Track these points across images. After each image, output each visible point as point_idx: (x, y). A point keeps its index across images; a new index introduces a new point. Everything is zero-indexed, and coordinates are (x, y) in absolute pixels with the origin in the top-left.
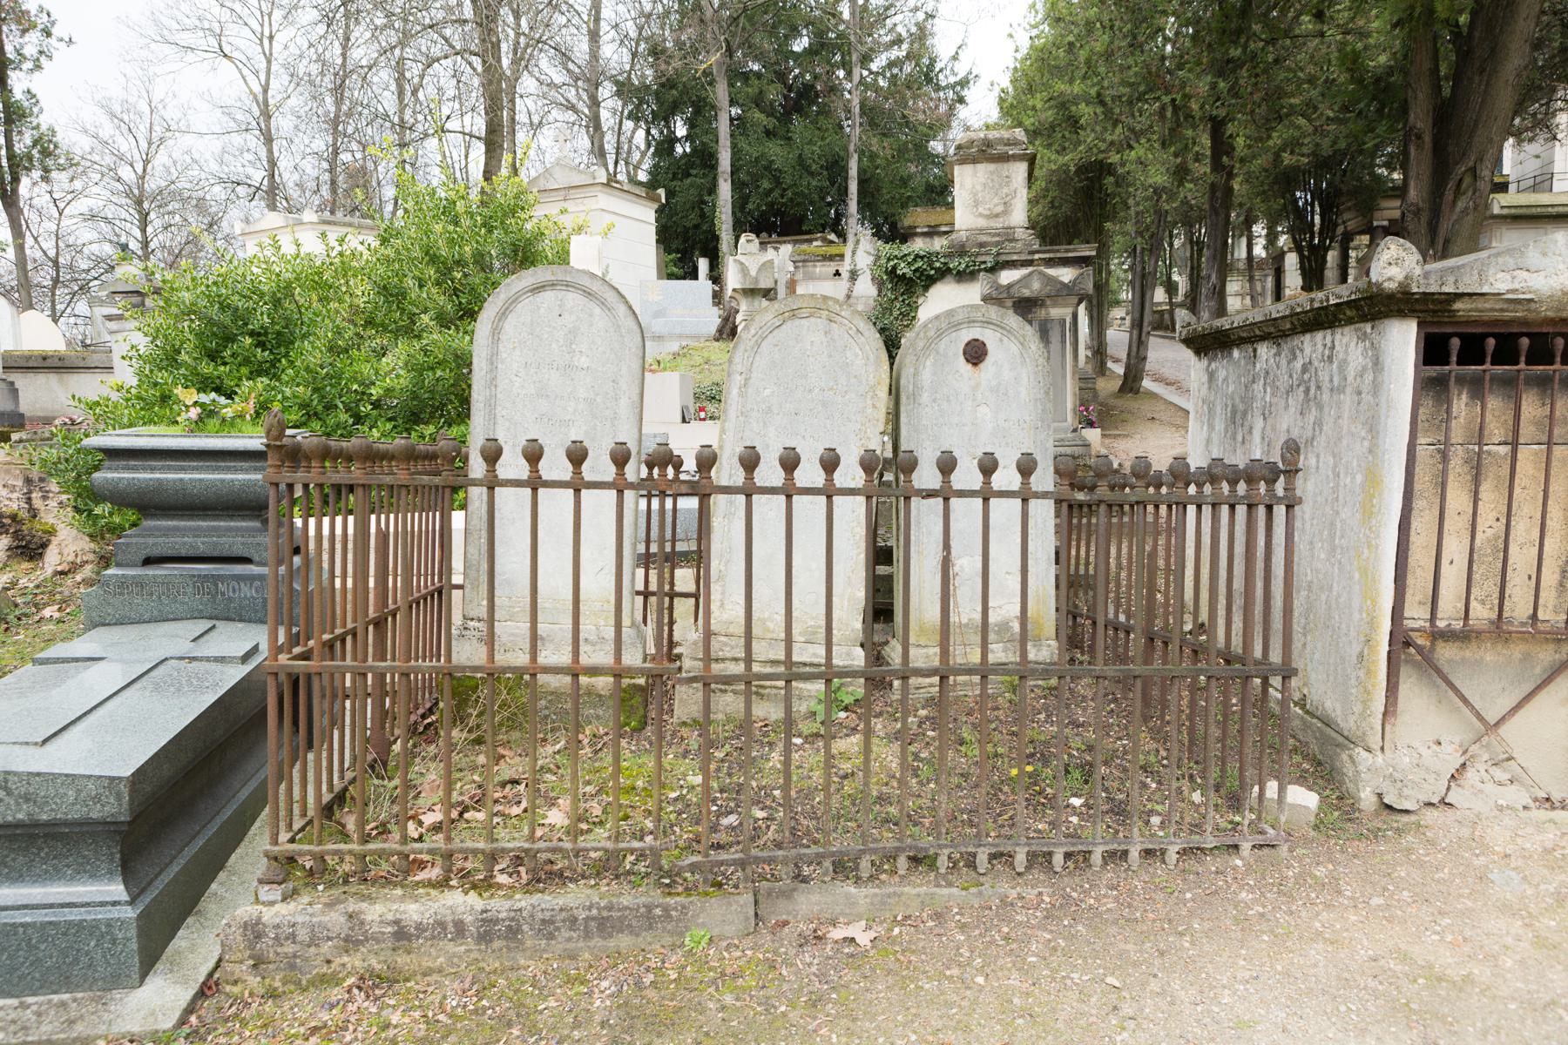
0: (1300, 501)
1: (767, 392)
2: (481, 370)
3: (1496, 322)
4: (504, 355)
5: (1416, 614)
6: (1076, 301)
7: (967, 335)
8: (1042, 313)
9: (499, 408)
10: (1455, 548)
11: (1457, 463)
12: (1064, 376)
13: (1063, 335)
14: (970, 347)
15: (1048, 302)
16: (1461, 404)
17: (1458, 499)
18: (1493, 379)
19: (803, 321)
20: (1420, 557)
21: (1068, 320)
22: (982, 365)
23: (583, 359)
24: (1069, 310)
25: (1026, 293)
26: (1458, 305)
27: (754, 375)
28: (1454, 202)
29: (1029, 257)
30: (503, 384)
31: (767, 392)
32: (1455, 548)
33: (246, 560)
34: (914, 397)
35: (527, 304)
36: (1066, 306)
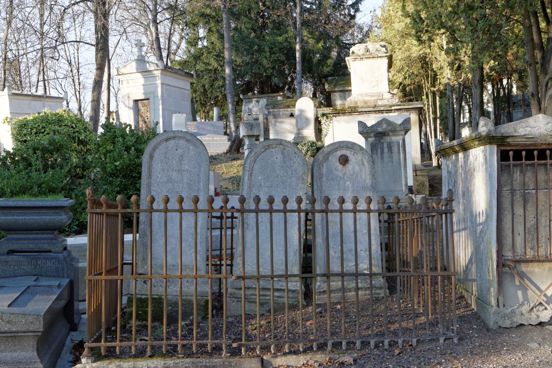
0: (454, 211)
1: (260, 178)
2: (145, 172)
3: (525, 145)
4: (154, 166)
5: (508, 254)
6: (404, 133)
7: (339, 153)
8: (387, 139)
9: (152, 187)
10: (520, 228)
11: (518, 197)
12: (400, 169)
13: (399, 149)
14: (341, 158)
15: (391, 134)
16: (517, 175)
17: (519, 211)
18: (527, 165)
19: (273, 150)
20: (508, 232)
21: (401, 142)
22: (347, 165)
23: (186, 166)
24: (401, 137)
25: (380, 130)
26: (508, 140)
27: (254, 171)
28: (546, 91)
29: (389, 109)
30: (154, 177)
31: (260, 178)
32: (520, 228)
33: (50, 252)
34: (321, 177)
35: (163, 145)
36: (399, 135)
